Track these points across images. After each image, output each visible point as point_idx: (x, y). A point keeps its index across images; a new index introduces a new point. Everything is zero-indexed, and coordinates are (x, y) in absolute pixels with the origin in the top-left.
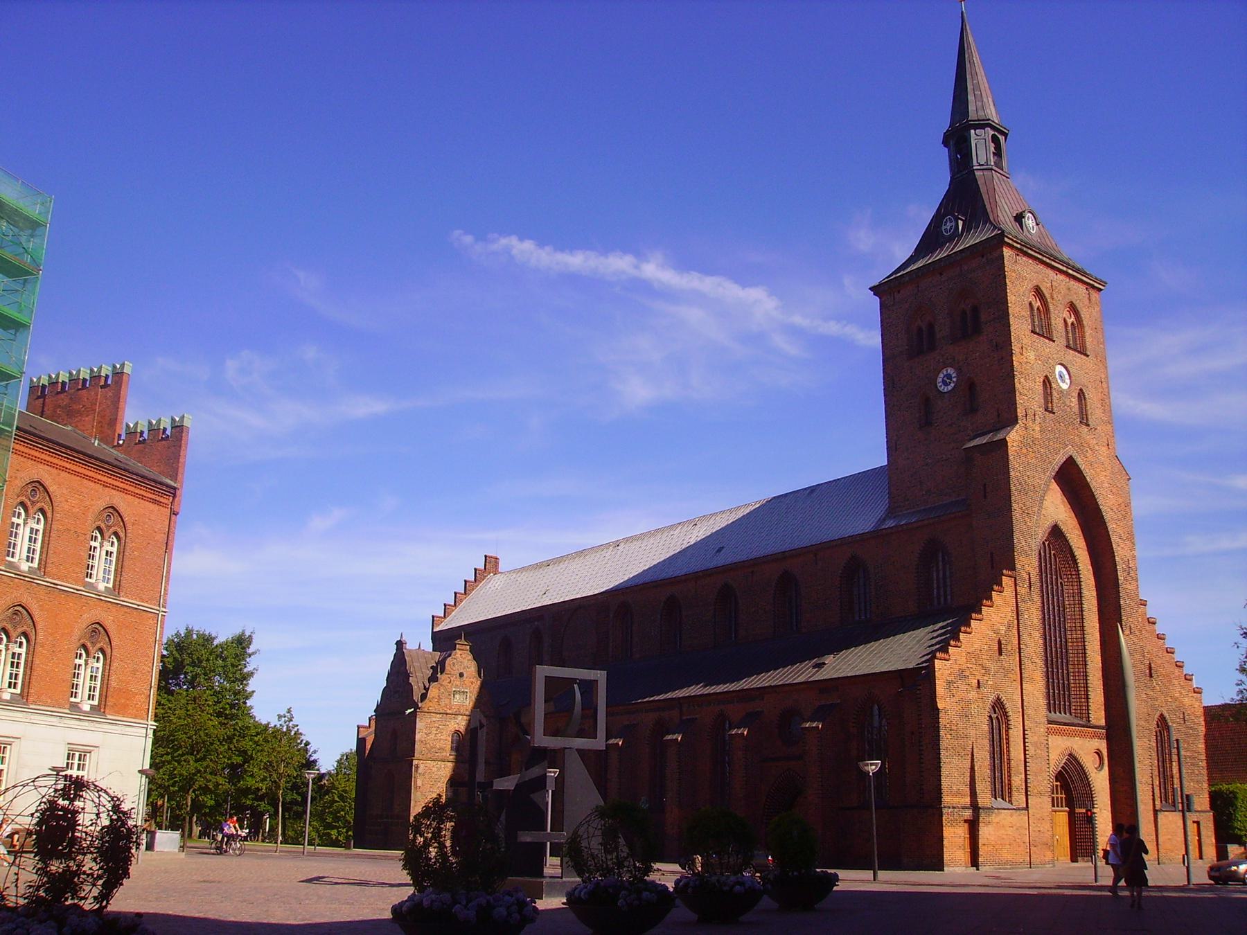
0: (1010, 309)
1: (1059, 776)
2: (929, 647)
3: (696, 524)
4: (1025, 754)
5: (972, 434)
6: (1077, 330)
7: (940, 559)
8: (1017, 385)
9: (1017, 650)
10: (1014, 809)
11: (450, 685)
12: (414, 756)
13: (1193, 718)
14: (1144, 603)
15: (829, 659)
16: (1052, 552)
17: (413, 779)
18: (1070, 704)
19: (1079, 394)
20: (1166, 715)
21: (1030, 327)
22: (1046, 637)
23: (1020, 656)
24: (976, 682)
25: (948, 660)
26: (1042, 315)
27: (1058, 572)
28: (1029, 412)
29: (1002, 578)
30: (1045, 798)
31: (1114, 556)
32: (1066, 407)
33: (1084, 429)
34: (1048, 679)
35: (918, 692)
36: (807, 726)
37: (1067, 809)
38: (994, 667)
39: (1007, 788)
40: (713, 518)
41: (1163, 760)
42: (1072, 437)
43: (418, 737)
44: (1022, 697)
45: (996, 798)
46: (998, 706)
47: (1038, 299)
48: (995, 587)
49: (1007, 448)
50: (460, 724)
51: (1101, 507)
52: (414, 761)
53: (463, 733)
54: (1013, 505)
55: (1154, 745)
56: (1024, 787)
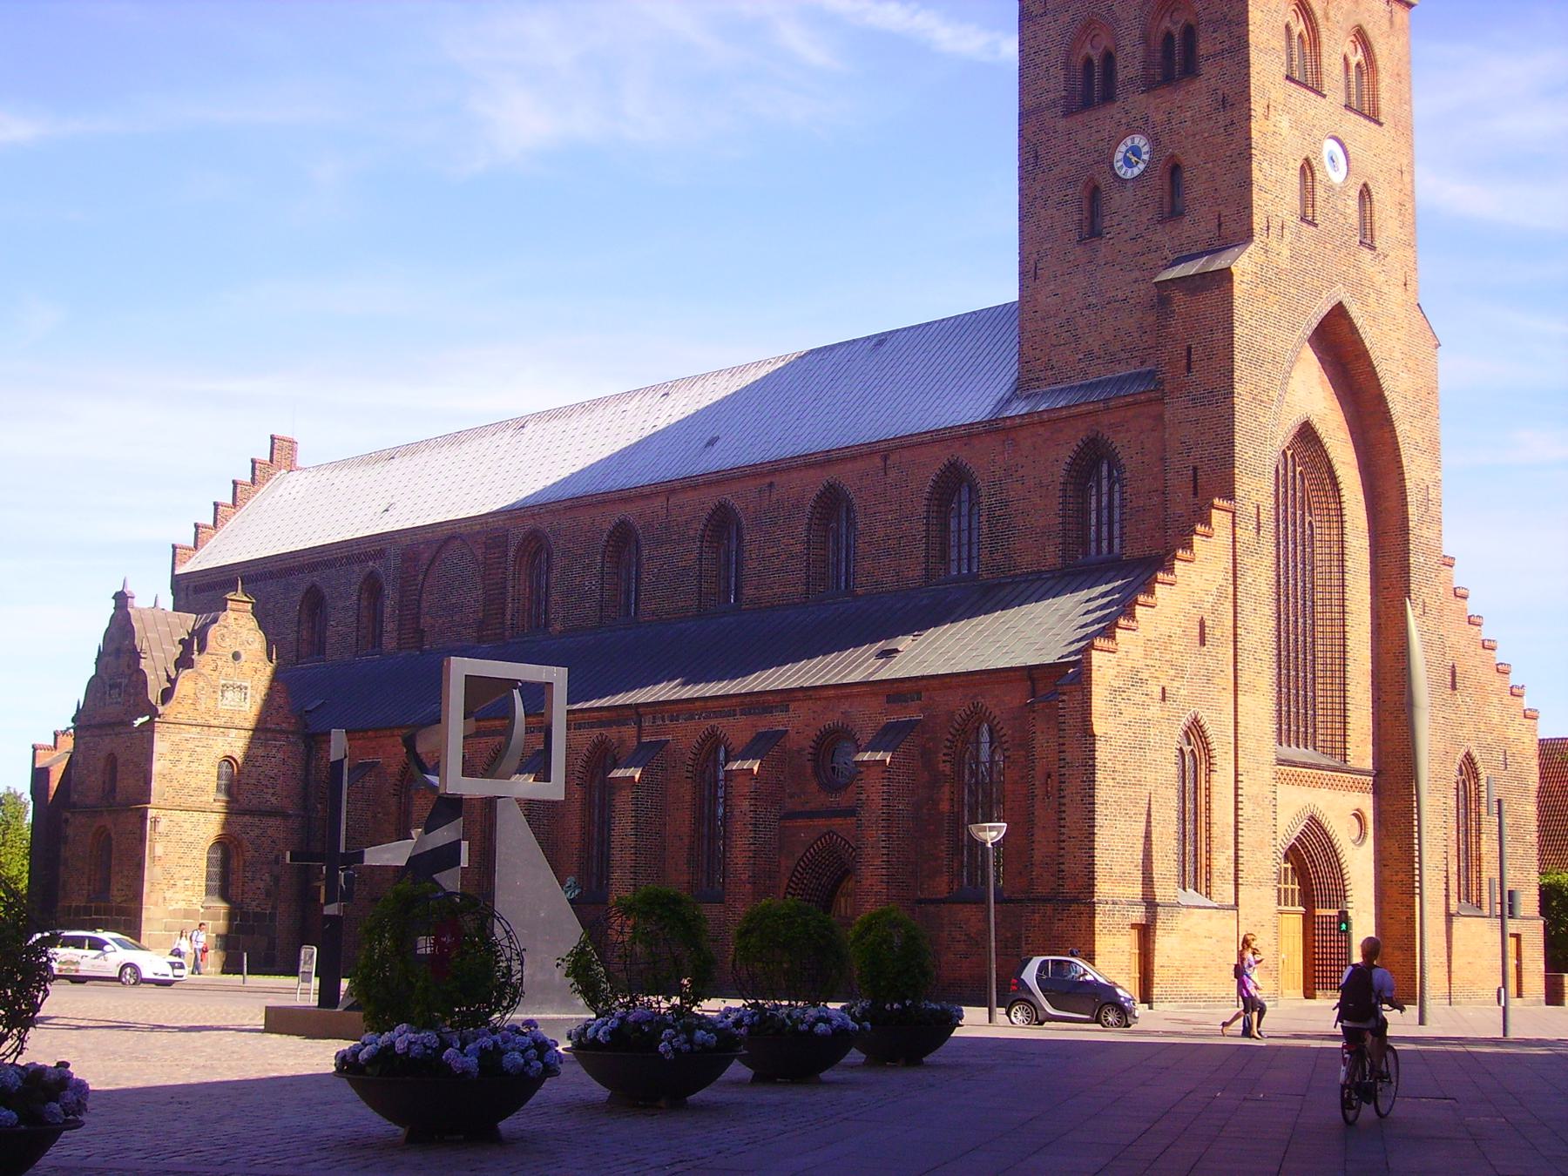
0: (1251, 36)
1: (1293, 854)
2: (1082, 627)
3: (667, 394)
4: (1236, 815)
5: (1171, 257)
6: (1365, 78)
7: (1105, 473)
8: (1256, 174)
9: (1232, 638)
10: (1216, 908)
11: (217, 673)
12: (149, 803)
13: (1520, 760)
14: (1449, 563)
15: (904, 643)
16: (1299, 469)
17: (147, 843)
18: (1315, 731)
19: (1361, 192)
20: (1475, 754)
21: (1284, 70)
22: (1279, 615)
23: (1235, 649)
25: (1114, 652)
26: (1307, 47)
27: (1306, 505)
28: (1276, 224)
29: (1211, 513)
30: (1266, 888)
31: (1404, 480)
32: (1337, 215)
33: (1366, 254)
34: (1280, 688)
35: (1061, 705)
36: (865, 759)
37: (1302, 909)
39: (1204, 871)
40: (700, 383)
41: (1466, 830)
42: (1344, 268)
43: (157, 767)
44: (1236, 719)
45: (1184, 889)
46: (1196, 733)
47: (1300, 15)
48: (1200, 528)
49: (1232, 286)
50: (236, 744)
51: (1386, 393)
52: (149, 810)
53: (239, 761)
54: (1236, 385)
55: (1453, 803)
56: (1232, 871)
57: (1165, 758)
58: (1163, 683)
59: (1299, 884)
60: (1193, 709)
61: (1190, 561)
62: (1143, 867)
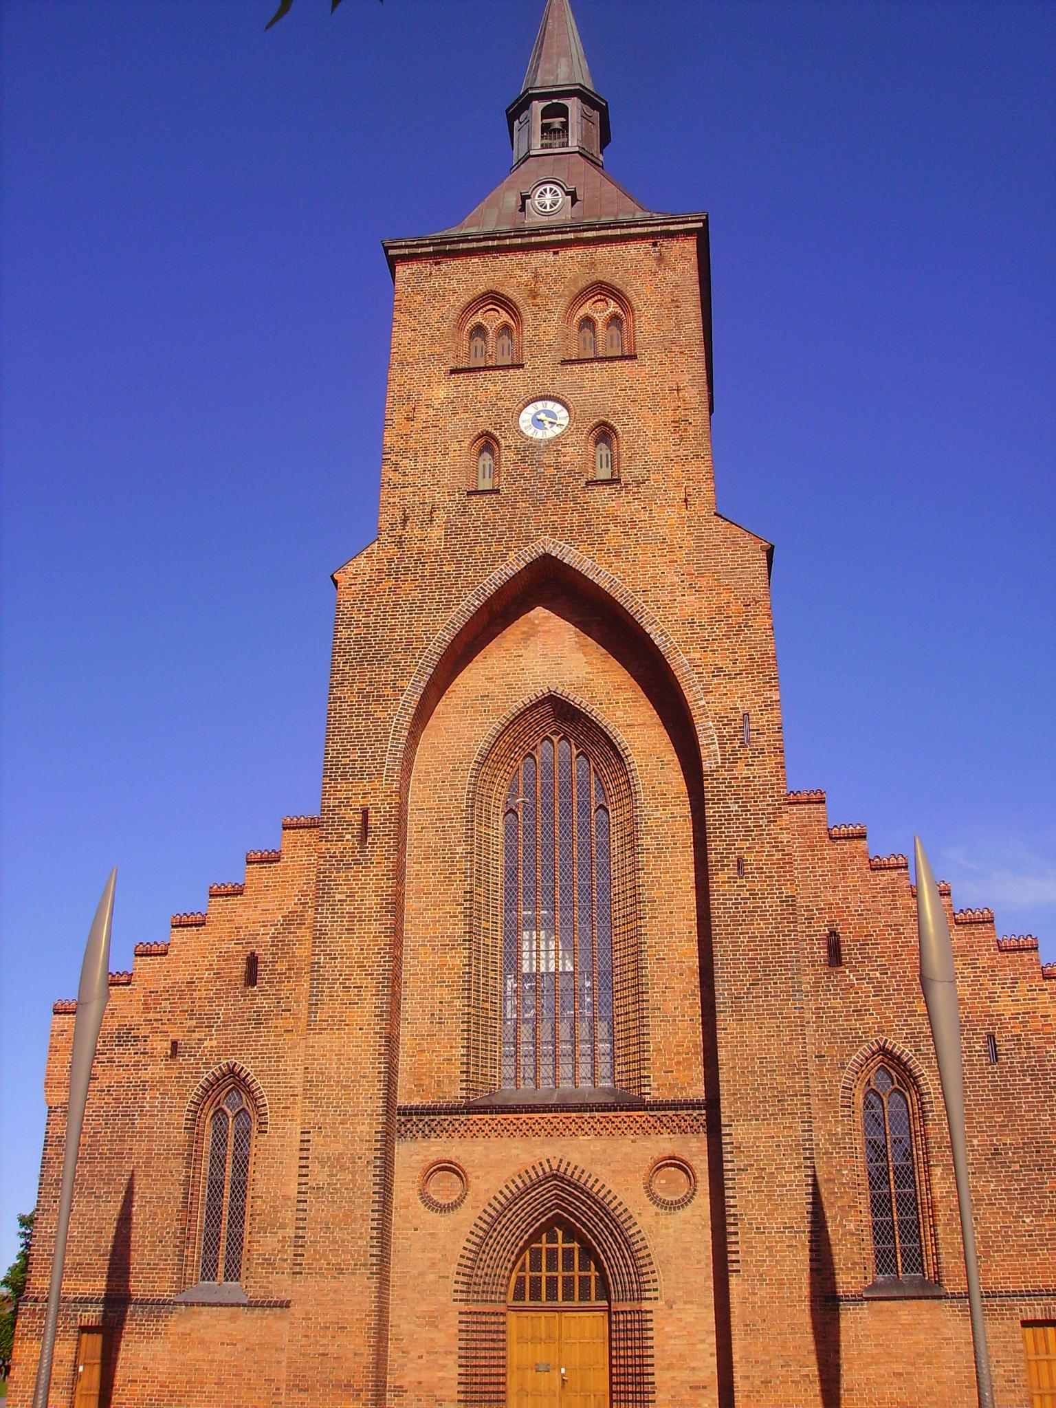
24: (168, 1044)
57: (167, 1124)
58: (172, 1037)
59: (596, 1270)
60: (225, 1062)
61: (237, 894)
62: (111, 1255)
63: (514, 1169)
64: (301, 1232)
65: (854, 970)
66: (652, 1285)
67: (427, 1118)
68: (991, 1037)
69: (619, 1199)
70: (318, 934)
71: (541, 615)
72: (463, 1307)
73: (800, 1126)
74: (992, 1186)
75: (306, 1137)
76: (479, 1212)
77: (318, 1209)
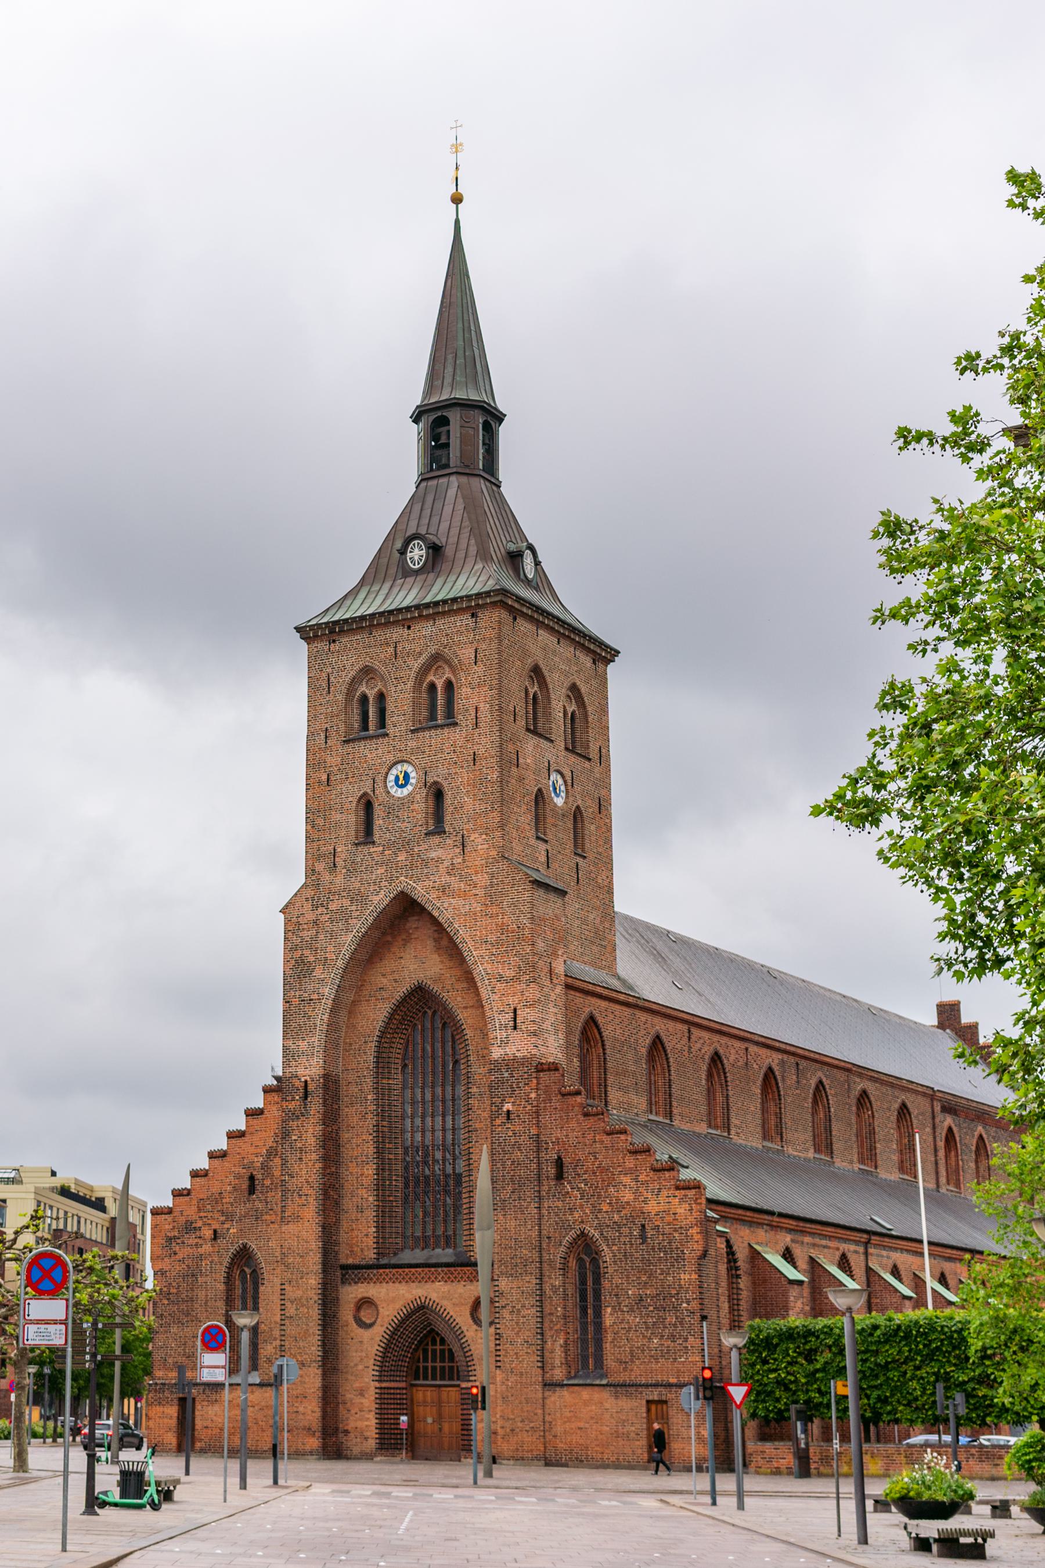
24: (211, 1232)
38: (240, 1210)
58: (213, 1227)
63: (402, 1303)
64: (283, 1343)
65: (569, 1183)
66: (474, 1373)
67: (356, 1272)
68: (643, 1226)
69: (457, 1321)
70: (284, 1162)
71: (414, 926)
72: (378, 1385)
73: (534, 1281)
74: (638, 1320)
75: (283, 1287)
76: (384, 1329)
77: (291, 1329)
